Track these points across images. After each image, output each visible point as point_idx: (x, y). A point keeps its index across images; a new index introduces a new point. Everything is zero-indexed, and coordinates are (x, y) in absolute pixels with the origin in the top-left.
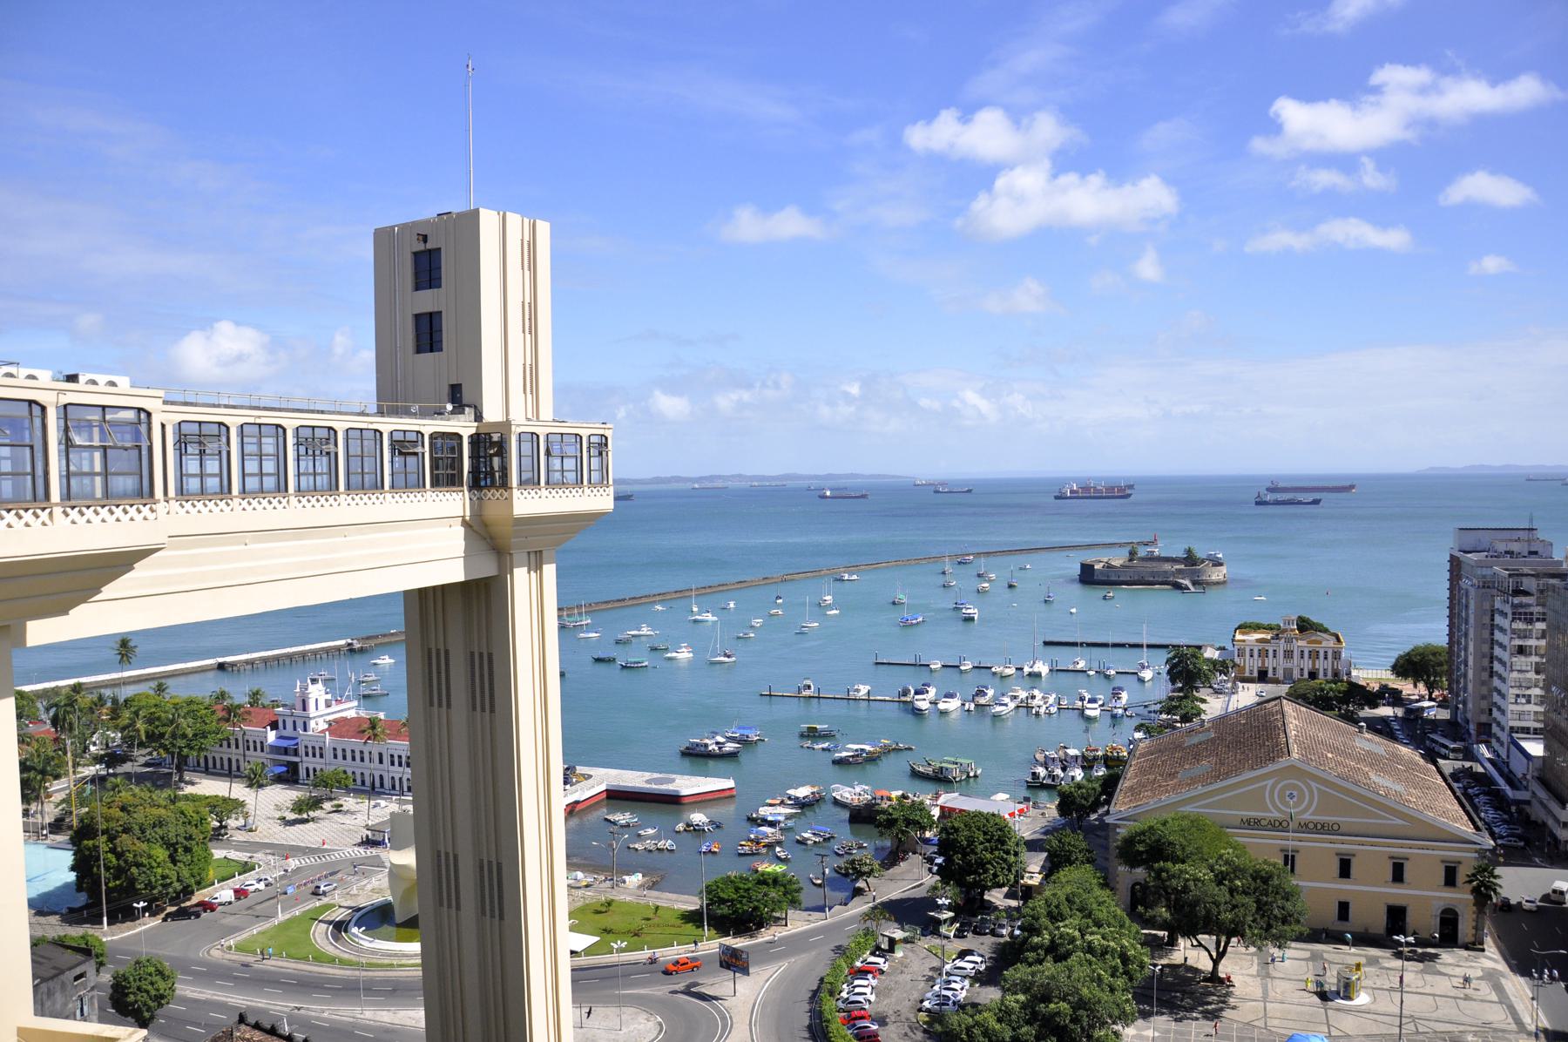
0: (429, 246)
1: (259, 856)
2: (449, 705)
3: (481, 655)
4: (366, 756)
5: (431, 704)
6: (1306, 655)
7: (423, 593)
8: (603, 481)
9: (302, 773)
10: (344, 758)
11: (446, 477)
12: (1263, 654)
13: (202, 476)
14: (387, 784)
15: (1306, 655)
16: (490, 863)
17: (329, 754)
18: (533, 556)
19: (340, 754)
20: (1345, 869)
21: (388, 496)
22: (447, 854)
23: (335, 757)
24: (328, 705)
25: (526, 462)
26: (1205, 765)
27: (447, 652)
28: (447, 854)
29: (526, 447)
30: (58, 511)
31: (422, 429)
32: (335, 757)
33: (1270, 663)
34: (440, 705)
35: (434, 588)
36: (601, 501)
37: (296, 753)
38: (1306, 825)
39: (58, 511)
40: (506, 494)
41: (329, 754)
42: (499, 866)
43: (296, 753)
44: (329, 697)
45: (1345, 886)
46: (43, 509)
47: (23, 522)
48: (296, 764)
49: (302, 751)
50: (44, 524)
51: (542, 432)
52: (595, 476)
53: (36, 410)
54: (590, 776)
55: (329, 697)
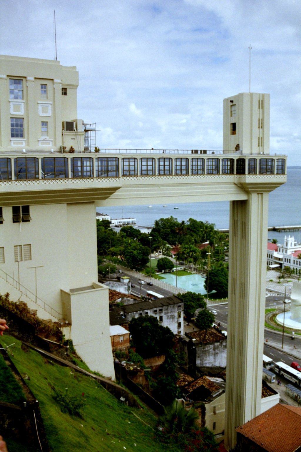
8: (283, 173)
9: (283, 268)
17: (292, 261)
18: (260, 195)
19: (296, 262)
24: (295, 245)
32: (294, 263)
41: (292, 261)
44: (296, 242)
47: (105, 181)
48: (281, 264)
50: (92, 182)
55: (296, 242)
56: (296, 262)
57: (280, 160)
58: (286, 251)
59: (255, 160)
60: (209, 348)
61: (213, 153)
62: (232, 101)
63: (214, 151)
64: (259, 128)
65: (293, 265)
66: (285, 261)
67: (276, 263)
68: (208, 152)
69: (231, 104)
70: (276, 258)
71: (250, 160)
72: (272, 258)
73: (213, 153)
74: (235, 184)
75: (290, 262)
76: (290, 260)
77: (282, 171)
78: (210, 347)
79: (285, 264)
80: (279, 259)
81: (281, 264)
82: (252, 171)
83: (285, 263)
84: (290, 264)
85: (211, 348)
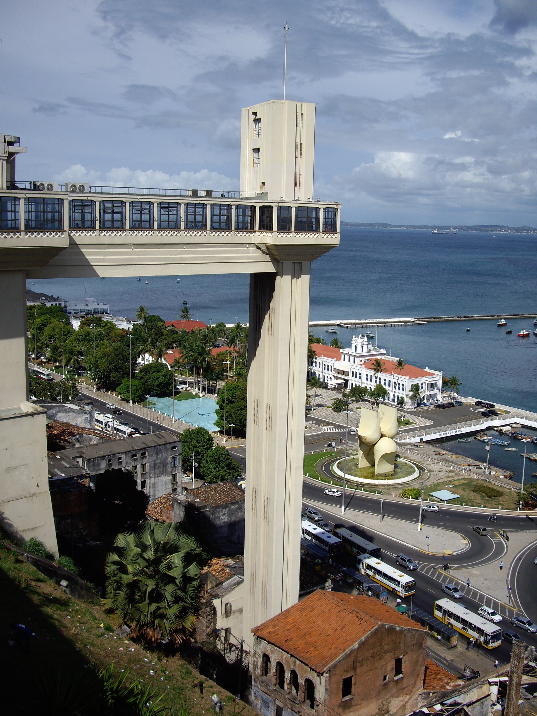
0: (258, 117)
4: (374, 379)
9: (349, 387)
11: (245, 226)
17: (364, 377)
18: (297, 265)
21: (209, 232)
23: (367, 379)
30: (23, 233)
31: (232, 203)
32: (367, 379)
36: (332, 239)
37: (348, 375)
41: (364, 377)
43: (348, 375)
48: (347, 381)
51: (294, 206)
54: (509, 412)
57: (330, 210)
59: (289, 208)
60: (221, 514)
61: (223, 196)
63: (223, 192)
64: (296, 157)
66: (353, 376)
67: (337, 378)
68: (214, 194)
70: (339, 371)
71: (280, 208)
73: (223, 196)
75: (360, 378)
76: (360, 374)
77: (330, 227)
78: (224, 513)
79: (353, 381)
80: (344, 373)
81: (347, 381)
82: (284, 227)
84: (360, 380)
85: (225, 514)
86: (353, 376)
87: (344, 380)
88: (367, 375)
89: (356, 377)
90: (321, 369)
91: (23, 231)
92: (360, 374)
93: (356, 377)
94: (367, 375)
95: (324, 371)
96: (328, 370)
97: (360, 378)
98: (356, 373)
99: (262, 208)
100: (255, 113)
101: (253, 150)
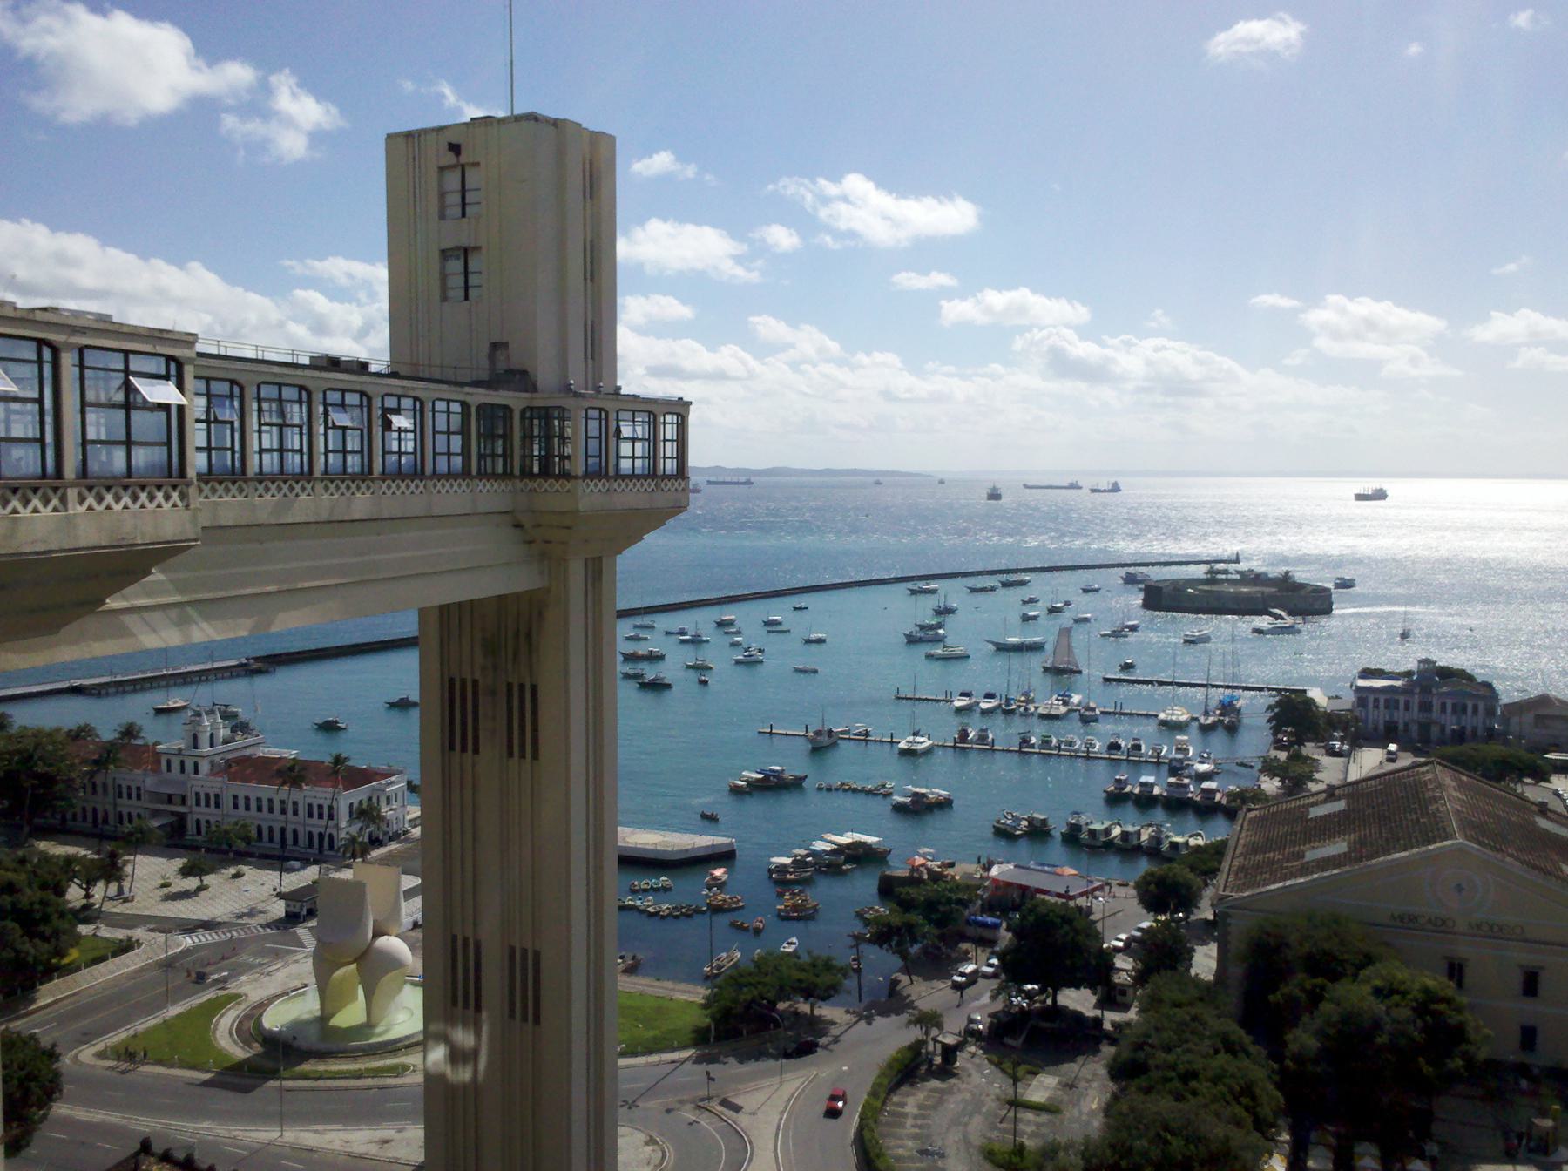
0: (463, 159)
1: (139, 933)
2: (476, 751)
3: (522, 687)
5: (452, 747)
6: (1449, 710)
7: (444, 610)
9: (191, 826)
10: (247, 808)
12: (1391, 705)
13: (282, 450)
14: (303, 840)
15: (1449, 710)
16: (524, 951)
17: (227, 802)
19: (241, 803)
20: (1531, 984)
22: (466, 940)
23: (236, 806)
25: (593, 444)
26: (1338, 847)
27: (475, 683)
28: (466, 940)
29: (594, 425)
31: (468, 399)
32: (236, 806)
33: (1400, 716)
34: (464, 749)
35: (460, 604)
37: (183, 801)
38: (1479, 926)
39: (72, 494)
40: (569, 485)
41: (227, 802)
42: (537, 955)
45: (1528, 1005)
46: (55, 489)
48: (182, 818)
49: (191, 801)
52: (670, 466)
53: (47, 354)
56: (241, 803)
58: (196, 765)
62: (455, 148)
65: (232, 812)
66: (198, 804)
69: (450, 158)
72: (139, 797)
74: (518, 526)
75: (217, 805)
76: (217, 796)
80: (170, 799)
81: (182, 818)
83: (196, 809)
86: (198, 804)
87: (173, 813)
88: (235, 797)
89: (207, 805)
90: (110, 798)
91: (73, 485)
92: (217, 796)
93: (207, 805)
94: (235, 797)
95: (119, 801)
96: (130, 796)
97: (217, 805)
98: (207, 796)
99: (529, 413)
100: (455, 148)
101: (445, 254)
